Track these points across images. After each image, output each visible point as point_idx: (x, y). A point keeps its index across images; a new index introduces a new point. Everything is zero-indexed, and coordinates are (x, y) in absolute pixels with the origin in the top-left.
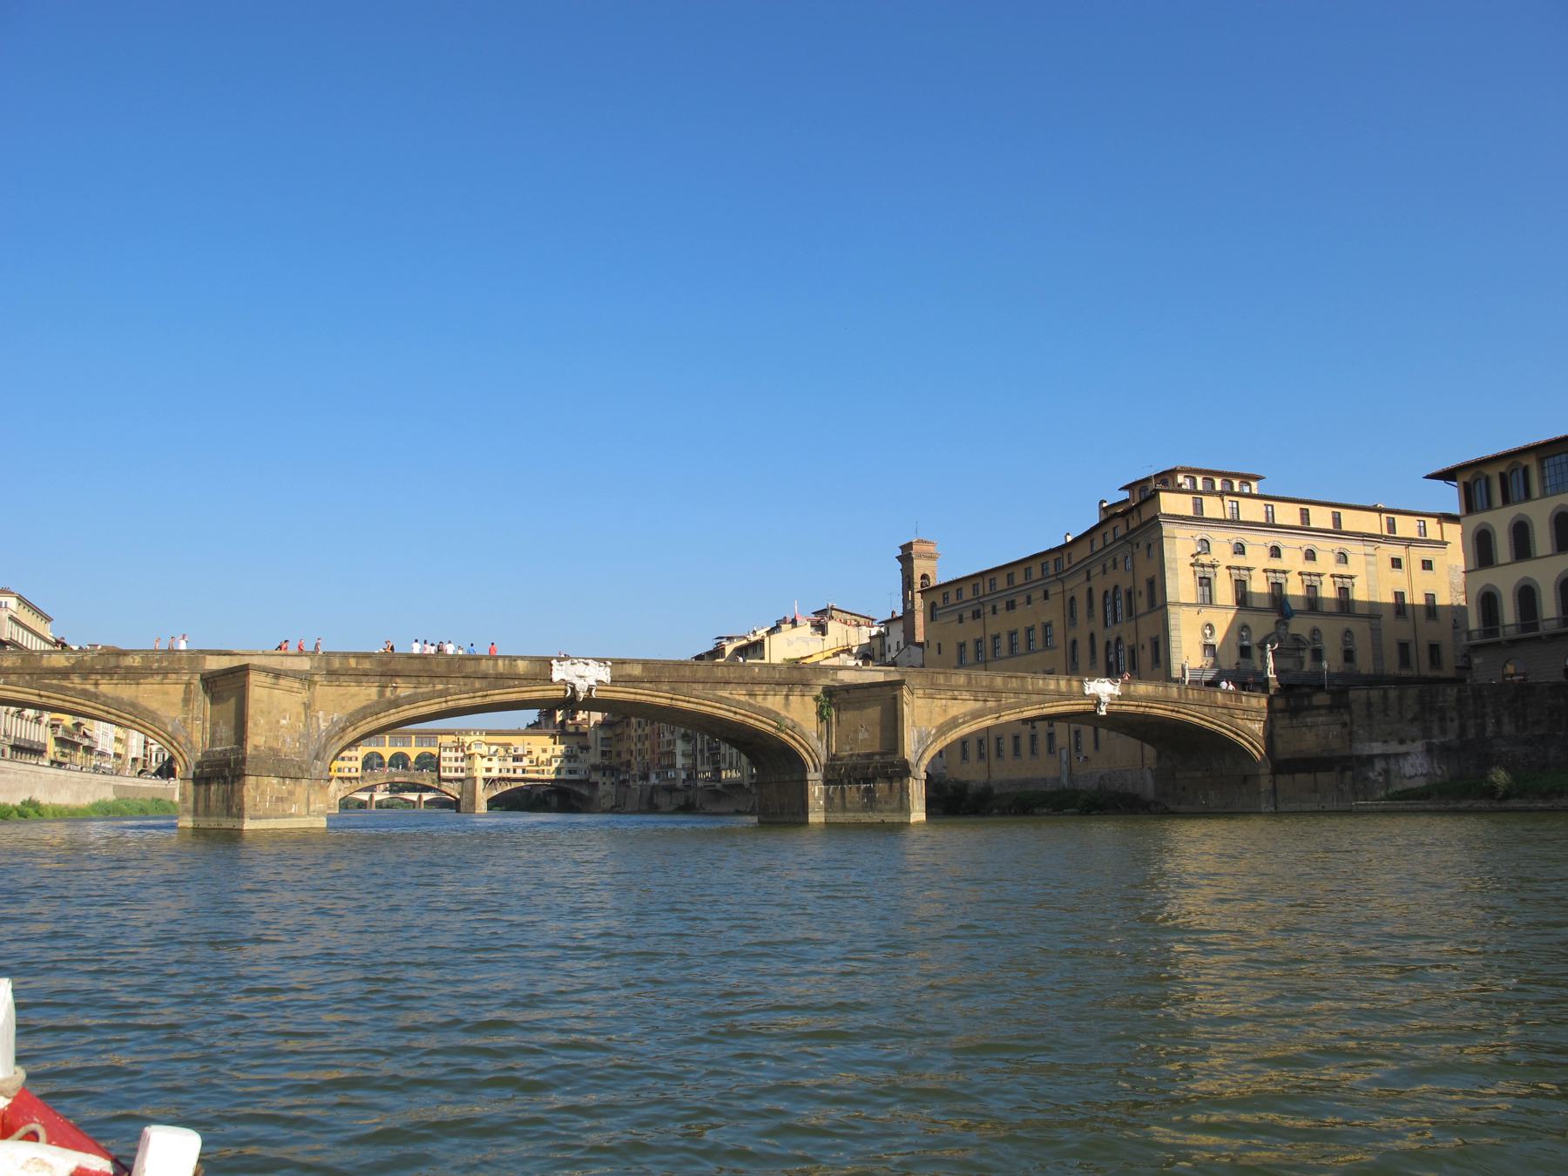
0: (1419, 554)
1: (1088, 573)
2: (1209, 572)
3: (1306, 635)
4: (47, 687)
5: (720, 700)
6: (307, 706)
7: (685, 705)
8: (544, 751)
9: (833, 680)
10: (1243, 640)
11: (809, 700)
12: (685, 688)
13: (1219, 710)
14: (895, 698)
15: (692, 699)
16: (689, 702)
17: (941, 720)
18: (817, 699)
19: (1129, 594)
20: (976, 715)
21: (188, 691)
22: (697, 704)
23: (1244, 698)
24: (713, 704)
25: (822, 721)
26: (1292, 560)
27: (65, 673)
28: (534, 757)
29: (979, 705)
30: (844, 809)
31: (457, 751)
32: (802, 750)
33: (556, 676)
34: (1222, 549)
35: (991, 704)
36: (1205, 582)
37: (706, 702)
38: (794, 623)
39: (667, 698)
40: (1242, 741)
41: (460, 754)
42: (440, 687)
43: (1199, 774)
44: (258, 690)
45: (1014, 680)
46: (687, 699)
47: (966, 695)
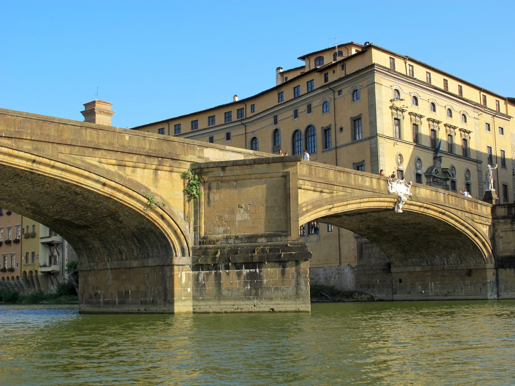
0: (499, 122)
1: (276, 118)
7: (48, 170)
9: (199, 157)
10: (417, 169)
11: (177, 176)
12: (49, 150)
13: (467, 214)
14: (286, 177)
15: (58, 164)
16: (53, 167)
18: (184, 176)
19: (326, 131)
22: (63, 170)
23: (479, 206)
24: (81, 172)
25: (189, 201)
30: (219, 296)
32: (169, 231)
37: (73, 169)
39: (28, 160)
40: (477, 240)
43: (418, 269)
45: (342, 174)
46: (52, 163)
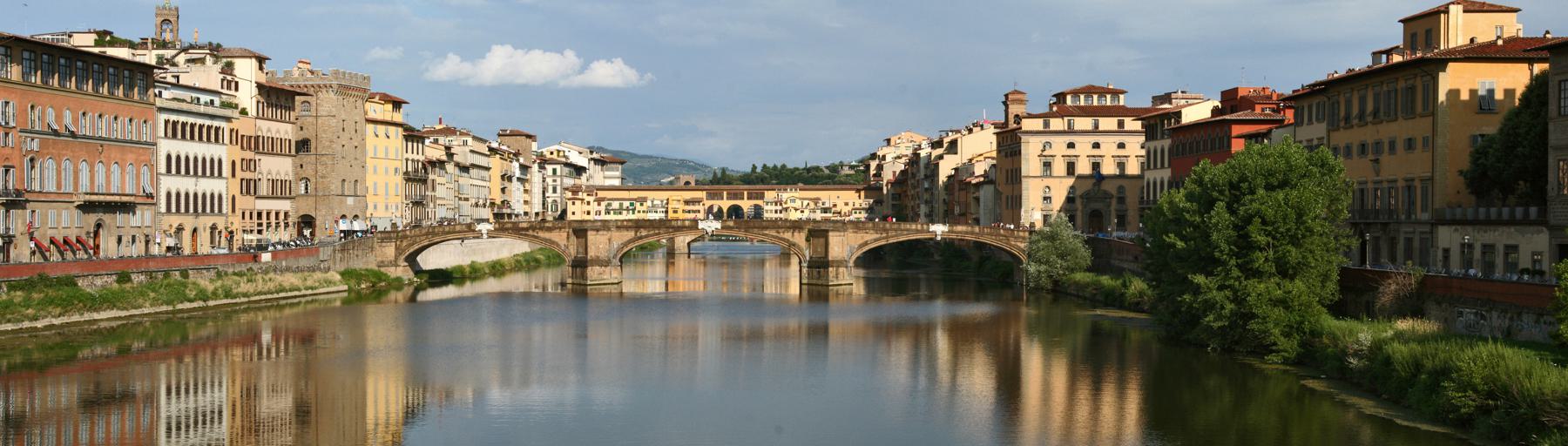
2: (1049, 159)
3: (1114, 192)
4: (521, 234)
5: (766, 235)
6: (609, 240)
8: (847, 204)
12: (751, 230)
17: (861, 242)
20: (876, 240)
21: (568, 235)
26: (1109, 146)
27: (527, 229)
28: (838, 209)
29: (878, 236)
31: (776, 205)
33: (700, 227)
34: (1059, 145)
35: (884, 235)
36: (1047, 165)
38: (982, 126)
41: (779, 208)
42: (657, 232)
44: (591, 235)
47: (872, 232)
